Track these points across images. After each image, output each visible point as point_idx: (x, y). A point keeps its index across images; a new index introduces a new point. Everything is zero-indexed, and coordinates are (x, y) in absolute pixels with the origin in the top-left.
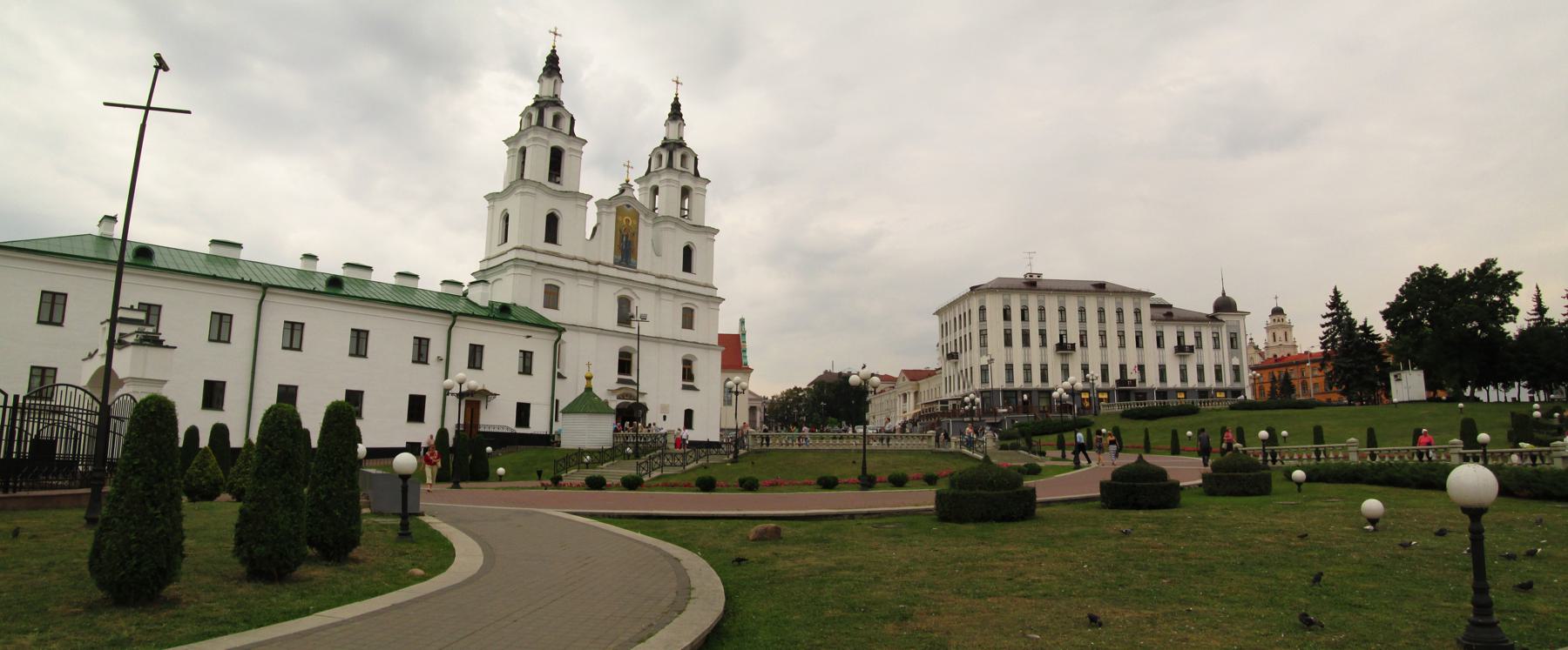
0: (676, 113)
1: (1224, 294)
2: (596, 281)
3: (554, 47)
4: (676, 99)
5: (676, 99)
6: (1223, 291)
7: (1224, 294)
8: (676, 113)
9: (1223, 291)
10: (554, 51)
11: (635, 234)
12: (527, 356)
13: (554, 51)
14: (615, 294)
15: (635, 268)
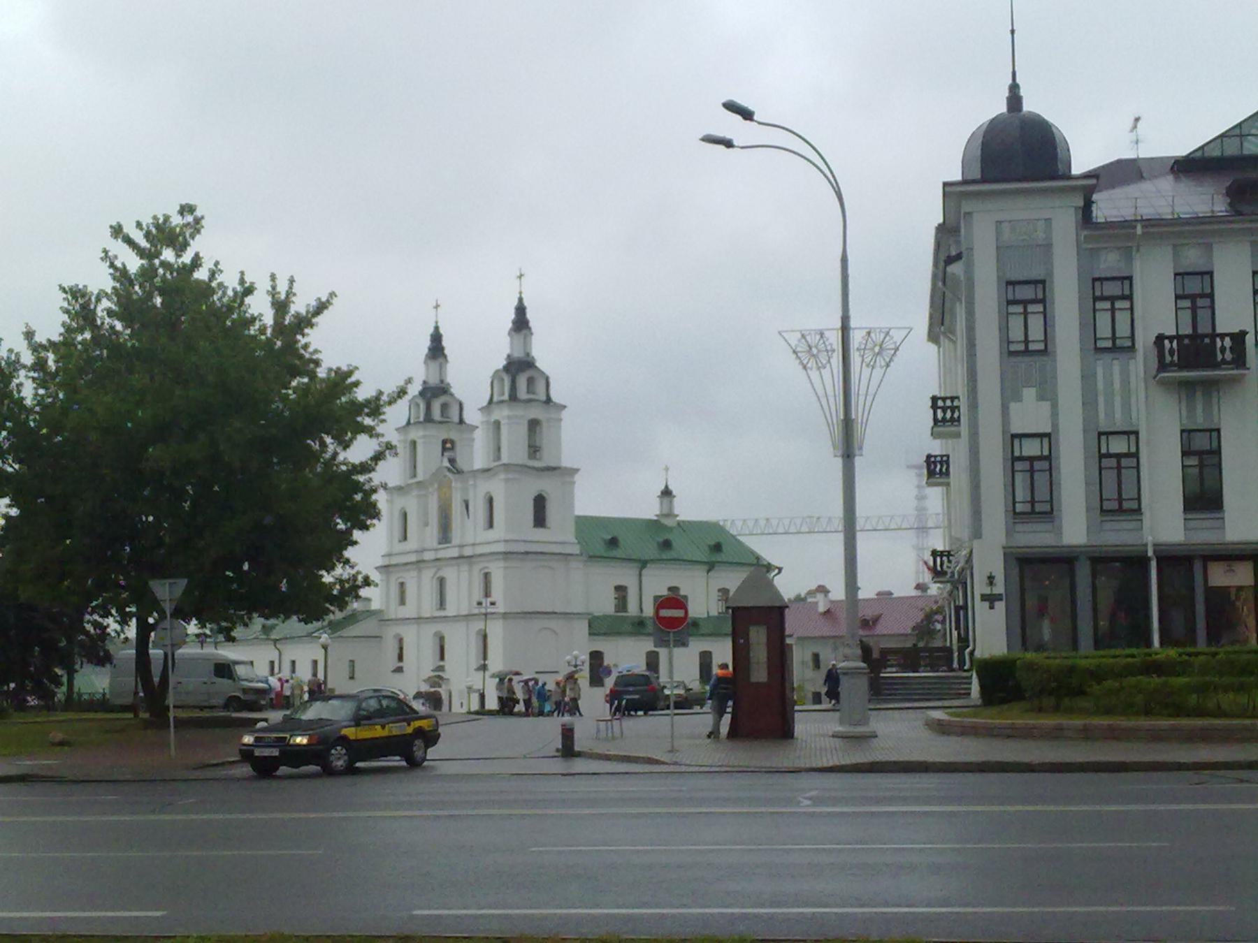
0: (521, 323)
1: (1015, 100)
2: (420, 570)
3: (437, 322)
4: (521, 300)
5: (521, 300)
6: (1014, 88)
7: (1015, 100)
8: (521, 323)
9: (1014, 88)
10: (437, 328)
11: (450, 506)
12: (315, 663)
13: (437, 328)
14: (433, 578)
15: (450, 542)
